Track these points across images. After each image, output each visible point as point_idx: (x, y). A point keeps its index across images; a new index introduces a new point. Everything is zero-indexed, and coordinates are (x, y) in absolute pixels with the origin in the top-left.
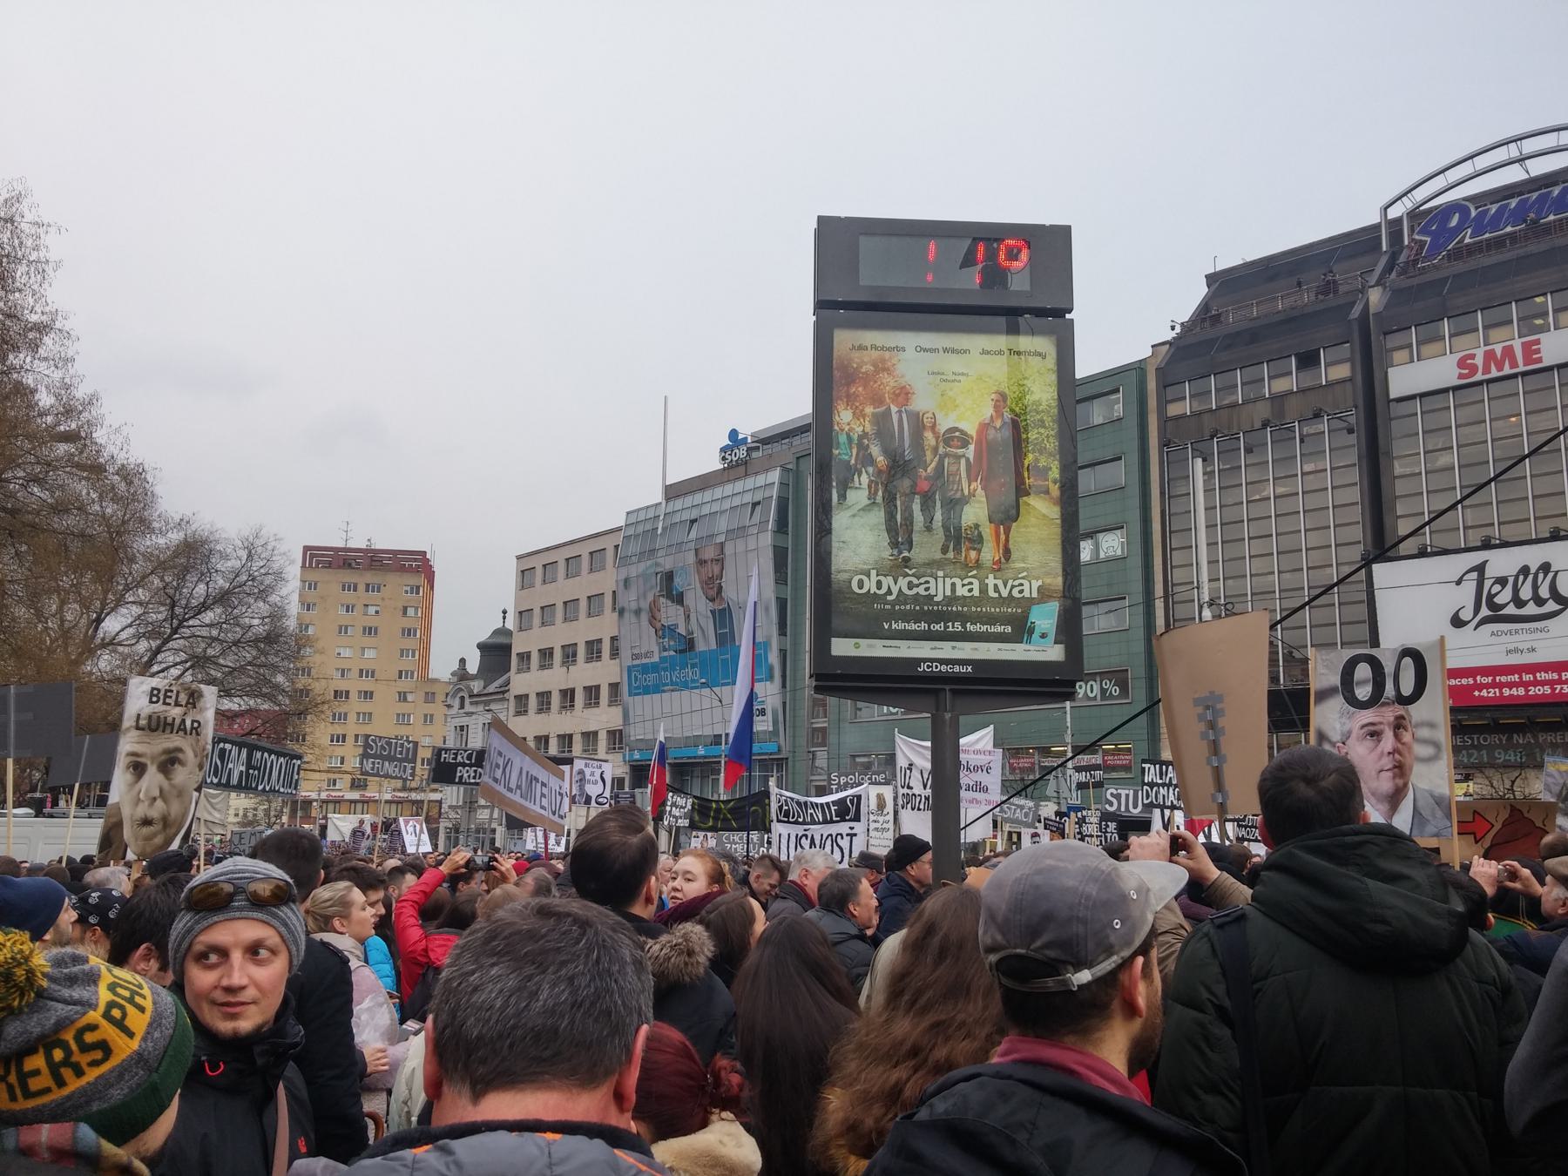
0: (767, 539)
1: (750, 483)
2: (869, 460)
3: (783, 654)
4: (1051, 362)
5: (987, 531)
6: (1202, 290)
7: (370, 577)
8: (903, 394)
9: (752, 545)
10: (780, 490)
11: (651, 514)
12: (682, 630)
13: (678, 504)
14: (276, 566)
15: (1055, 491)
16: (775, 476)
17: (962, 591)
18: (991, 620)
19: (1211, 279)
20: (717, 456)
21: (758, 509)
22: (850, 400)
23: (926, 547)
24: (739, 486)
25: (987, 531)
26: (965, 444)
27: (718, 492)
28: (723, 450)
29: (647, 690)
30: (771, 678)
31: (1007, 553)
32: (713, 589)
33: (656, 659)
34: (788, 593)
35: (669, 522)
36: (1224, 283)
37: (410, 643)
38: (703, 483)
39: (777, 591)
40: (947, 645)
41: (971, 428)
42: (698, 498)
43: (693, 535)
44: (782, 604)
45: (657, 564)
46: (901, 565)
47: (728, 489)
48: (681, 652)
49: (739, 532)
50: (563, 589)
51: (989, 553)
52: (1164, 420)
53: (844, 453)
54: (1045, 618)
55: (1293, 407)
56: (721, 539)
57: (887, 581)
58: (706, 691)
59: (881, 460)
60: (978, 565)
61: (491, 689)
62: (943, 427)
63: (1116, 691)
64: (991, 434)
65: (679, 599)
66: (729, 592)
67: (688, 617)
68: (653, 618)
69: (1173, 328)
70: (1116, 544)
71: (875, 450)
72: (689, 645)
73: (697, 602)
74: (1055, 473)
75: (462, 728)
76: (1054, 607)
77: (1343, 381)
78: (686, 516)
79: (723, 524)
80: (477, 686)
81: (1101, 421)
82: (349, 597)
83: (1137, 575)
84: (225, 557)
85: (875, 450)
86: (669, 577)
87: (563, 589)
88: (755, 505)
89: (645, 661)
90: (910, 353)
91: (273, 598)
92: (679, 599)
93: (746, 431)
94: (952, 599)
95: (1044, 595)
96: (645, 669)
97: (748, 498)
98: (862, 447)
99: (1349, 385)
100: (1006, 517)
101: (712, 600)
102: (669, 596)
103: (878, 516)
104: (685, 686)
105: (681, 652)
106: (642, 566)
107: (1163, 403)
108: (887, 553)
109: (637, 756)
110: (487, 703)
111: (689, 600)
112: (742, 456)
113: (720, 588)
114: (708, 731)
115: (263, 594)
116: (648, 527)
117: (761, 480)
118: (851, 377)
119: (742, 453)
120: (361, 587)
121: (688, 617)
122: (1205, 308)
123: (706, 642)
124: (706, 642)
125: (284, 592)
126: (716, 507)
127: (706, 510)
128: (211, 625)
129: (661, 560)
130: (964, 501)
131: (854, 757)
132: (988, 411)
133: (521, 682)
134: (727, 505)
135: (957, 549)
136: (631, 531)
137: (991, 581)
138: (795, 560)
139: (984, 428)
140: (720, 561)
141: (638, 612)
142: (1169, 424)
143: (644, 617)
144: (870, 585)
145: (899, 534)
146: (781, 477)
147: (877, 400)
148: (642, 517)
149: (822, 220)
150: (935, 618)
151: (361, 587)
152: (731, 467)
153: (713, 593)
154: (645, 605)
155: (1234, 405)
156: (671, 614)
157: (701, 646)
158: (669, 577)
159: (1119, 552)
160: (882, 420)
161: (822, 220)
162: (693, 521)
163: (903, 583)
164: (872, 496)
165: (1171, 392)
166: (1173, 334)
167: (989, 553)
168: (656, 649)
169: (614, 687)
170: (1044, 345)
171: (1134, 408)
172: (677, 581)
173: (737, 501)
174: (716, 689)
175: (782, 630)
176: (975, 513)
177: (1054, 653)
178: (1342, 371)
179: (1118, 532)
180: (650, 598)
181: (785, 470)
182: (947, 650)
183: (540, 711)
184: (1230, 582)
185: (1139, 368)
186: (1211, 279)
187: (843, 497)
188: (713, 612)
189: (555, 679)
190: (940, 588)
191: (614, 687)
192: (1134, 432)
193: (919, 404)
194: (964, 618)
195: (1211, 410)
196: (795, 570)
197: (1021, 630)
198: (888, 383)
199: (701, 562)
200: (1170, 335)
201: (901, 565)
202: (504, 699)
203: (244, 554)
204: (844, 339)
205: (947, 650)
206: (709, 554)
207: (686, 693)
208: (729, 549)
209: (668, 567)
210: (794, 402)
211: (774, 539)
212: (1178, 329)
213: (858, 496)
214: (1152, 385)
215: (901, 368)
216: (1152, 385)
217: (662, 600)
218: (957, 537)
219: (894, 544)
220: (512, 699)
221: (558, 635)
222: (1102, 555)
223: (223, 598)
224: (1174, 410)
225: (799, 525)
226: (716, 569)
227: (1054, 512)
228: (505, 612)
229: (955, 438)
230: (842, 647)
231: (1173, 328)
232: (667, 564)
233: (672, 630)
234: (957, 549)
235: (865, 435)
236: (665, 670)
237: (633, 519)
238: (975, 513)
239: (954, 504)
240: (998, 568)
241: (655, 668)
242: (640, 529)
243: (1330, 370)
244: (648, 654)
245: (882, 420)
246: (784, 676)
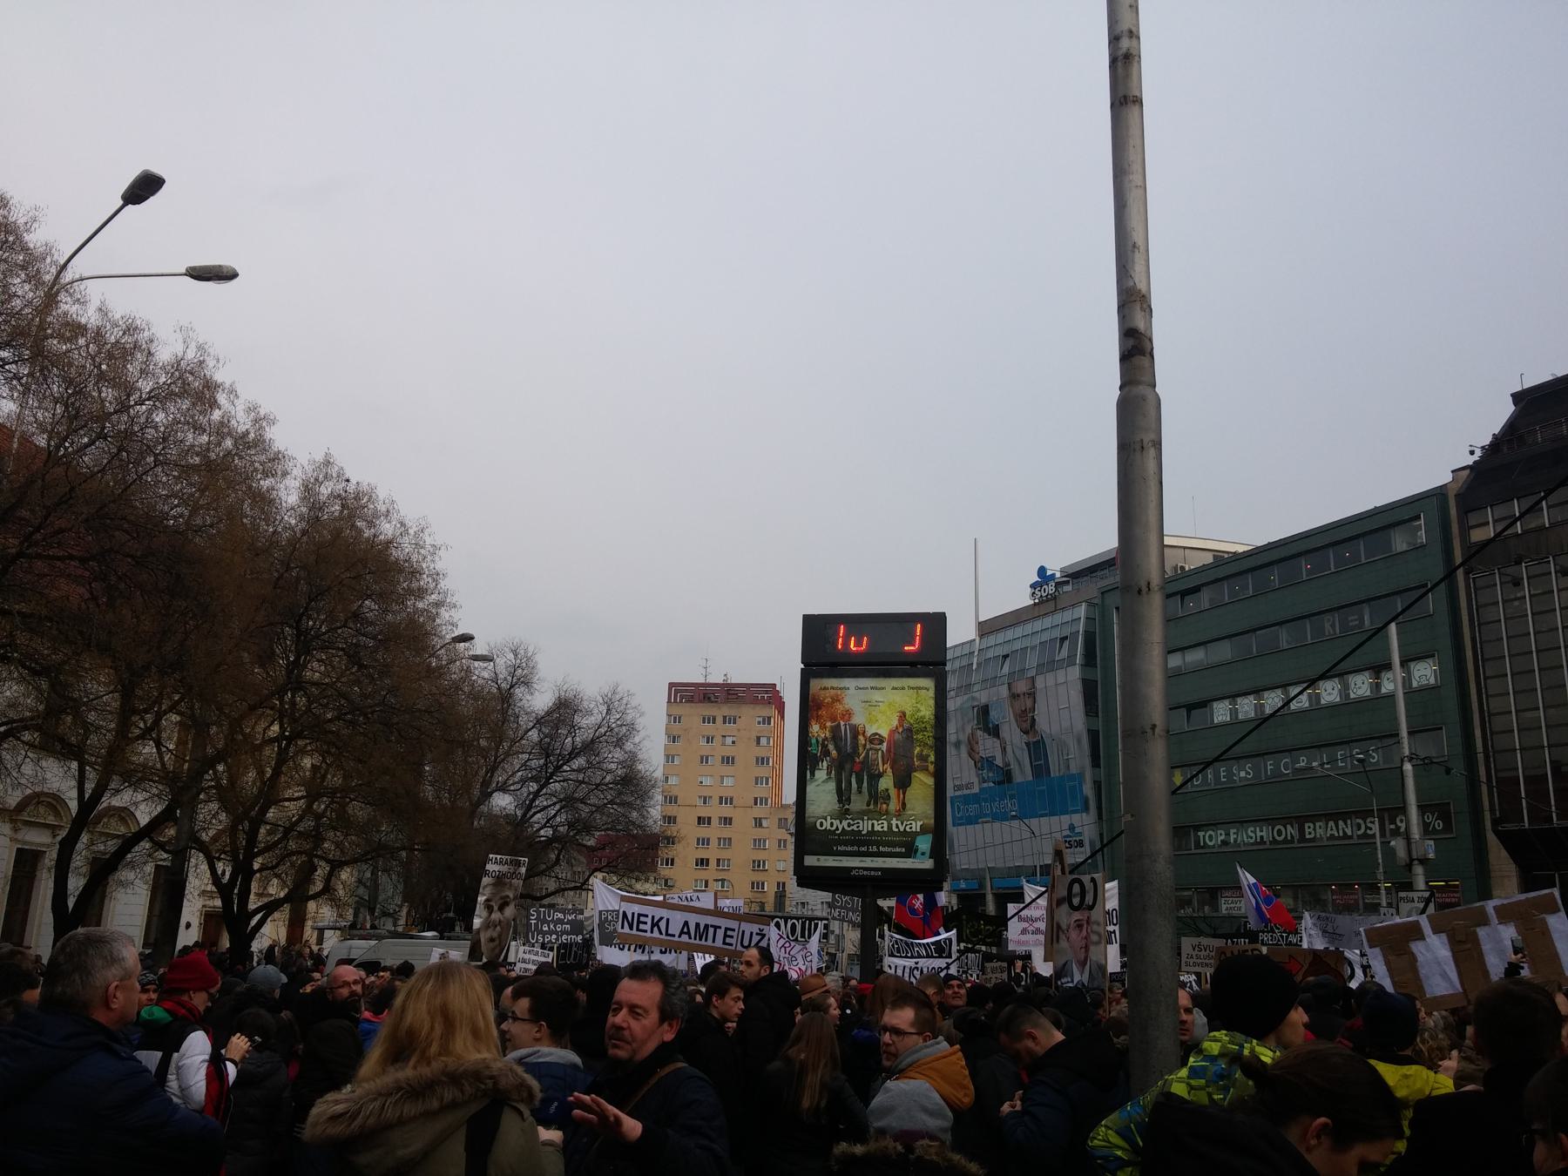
0: (1075, 673)
1: (1058, 618)
2: (826, 753)
3: (1097, 785)
4: (931, 693)
5: (893, 792)
6: (1502, 412)
7: (726, 710)
8: (848, 714)
9: (1061, 679)
10: (1086, 624)
12: (999, 762)
13: (991, 640)
14: (629, 718)
15: (931, 768)
16: (1082, 611)
17: (877, 828)
18: (893, 845)
19: (1517, 398)
20: (1029, 590)
21: (1067, 643)
22: (818, 718)
23: (858, 803)
24: (1048, 622)
25: (893, 792)
26: (881, 742)
27: (1028, 628)
28: (1033, 586)
29: (971, 821)
30: (1086, 809)
31: (904, 805)
32: (1028, 723)
33: (976, 790)
34: (1100, 725)
36: (1532, 402)
37: (763, 771)
38: (1015, 618)
40: (868, 859)
41: (885, 733)
42: (1009, 634)
43: (1006, 669)
44: (1093, 736)
45: (973, 699)
46: (843, 814)
47: (1038, 625)
48: (1000, 783)
49: (1049, 666)
51: (893, 805)
53: (815, 750)
54: (924, 844)
56: (1032, 673)
57: (837, 822)
58: (1015, 823)
59: (834, 753)
60: (887, 813)
62: (868, 734)
63: (1439, 825)
64: (897, 736)
65: (995, 732)
66: (1042, 724)
67: (1004, 750)
68: (972, 752)
69: (1472, 453)
70: (1428, 672)
71: (831, 747)
72: (1006, 776)
73: (1012, 733)
74: (932, 758)
76: (929, 838)
78: (1000, 651)
79: (1032, 661)
81: (1404, 547)
82: (709, 729)
84: (590, 713)
85: (831, 747)
86: (984, 711)
88: (1063, 639)
89: (966, 792)
90: (852, 691)
91: (629, 746)
92: (995, 732)
93: (1055, 567)
94: (872, 832)
95: (924, 830)
96: (966, 800)
97: (1057, 634)
98: (824, 746)
100: (903, 783)
101: (1026, 732)
102: (987, 730)
103: (832, 785)
104: (1002, 817)
105: (1000, 783)
106: (959, 701)
107: (1465, 530)
108: (837, 806)
109: (963, 885)
111: (1005, 732)
112: (1052, 590)
113: (1034, 720)
114: (1029, 862)
115: (619, 743)
117: (1068, 616)
118: (819, 706)
119: (1051, 588)
120: (719, 720)
121: (1004, 750)
122: (1511, 427)
123: (1023, 774)
124: (1023, 774)
125: (637, 740)
126: (1027, 643)
127: (1017, 646)
128: (579, 770)
129: (977, 695)
130: (880, 775)
132: (895, 723)
134: (1036, 641)
135: (876, 803)
137: (894, 822)
139: (892, 732)
140: (1032, 695)
141: (957, 744)
143: (964, 750)
144: (827, 825)
145: (843, 795)
146: (1087, 611)
147: (833, 719)
149: (806, 618)
150: (862, 843)
151: (719, 720)
152: (1041, 602)
153: (1027, 725)
154: (964, 737)
155: (1542, 528)
156: (988, 746)
157: (1018, 778)
158: (984, 711)
159: (1432, 681)
160: (835, 730)
161: (806, 618)
162: (1005, 657)
163: (845, 823)
164: (829, 773)
165: (1473, 519)
166: (1476, 457)
167: (893, 805)
168: (975, 780)
170: (928, 683)
172: (993, 714)
173: (1046, 637)
174: (1034, 822)
175: (1095, 762)
176: (887, 783)
177: (928, 864)
179: (1430, 661)
180: (968, 730)
181: (1090, 604)
182: (869, 862)
184: (1552, 711)
185: (1439, 493)
186: (1517, 398)
187: (813, 774)
188: (1027, 744)
190: (865, 826)
193: (857, 720)
194: (878, 844)
195: (1517, 535)
197: (911, 851)
198: (840, 708)
199: (1014, 697)
200: (1470, 460)
201: (843, 814)
203: (604, 709)
204: (816, 684)
205: (869, 862)
206: (1021, 687)
207: (997, 825)
208: (1039, 683)
209: (984, 701)
210: (1103, 538)
211: (1082, 671)
212: (1478, 453)
213: (821, 774)
214: (1453, 512)
215: (846, 700)
216: (1453, 512)
217: (979, 733)
218: (876, 797)
219: (840, 801)
222: (1415, 684)
223: (590, 747)
224: (1478, 535)
225: (1108, 657)
226: (1029, 703)
227: (930, 781)
229: (876, 739)
230: (810, 861)
231: (1472, 453)
232: (983, 697)
233: (990, 762)
234: (876, 803)
235: (826, 739)
236: (986, 800)
238: (887, 783)
239: (875, 777)
240: (899, 815)
241: (975, 798)
244: (969, 785)
245: (835, 730)
246: (1099, 808)
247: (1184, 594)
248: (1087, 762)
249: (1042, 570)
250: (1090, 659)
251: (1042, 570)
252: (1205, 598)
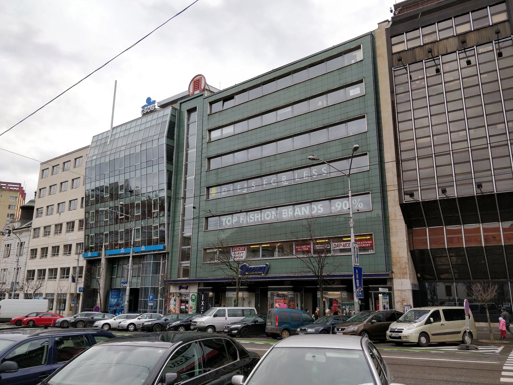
10: (171, 118)
11: (105, 136)
19: (396, 6)
28: (143, 107)
35: (112, 138)
39: (167, 167)
44: (170, 174)
50: (60, 176)
52: (391, 54)
55: (471, 39)
61: (24, 226)
75: (8, 245)
77: (504, 22)
80: (17, 225)
83: (374, 140)
87: (60, 176)
99: (507, 23)
107: (390, 46)
110: (21, 233)
116: (103, 141)
131: (205, 250)
133: (37, 222)
134: (143, 127)
136: (94, 145)
138: (178, 153)
142: (394, 56)
148: (100, 138)
165: (394, 40)
169: (81, 221)
171: (370, 54)
175: (169, 187)
178: (503, 17)
183: (45, 235)
185: (371, 35)
189: (53, 219)
191: (81, 221)
192: (371, 66)
195: (420, 46)
196: (178, 157)
202: (28, 231)
211: (167, 141)
220: (32, 230)
221: (56, 198)
224: (396, 49)
228: (36, 193)
237: (96, 139)
242: (99, 143)
243: (494, 17)
247: (226, 99)
248: (165, 186)
249: (149, 100)
250: (170, 135)
251: (149, 100)
252: (238, 99)
